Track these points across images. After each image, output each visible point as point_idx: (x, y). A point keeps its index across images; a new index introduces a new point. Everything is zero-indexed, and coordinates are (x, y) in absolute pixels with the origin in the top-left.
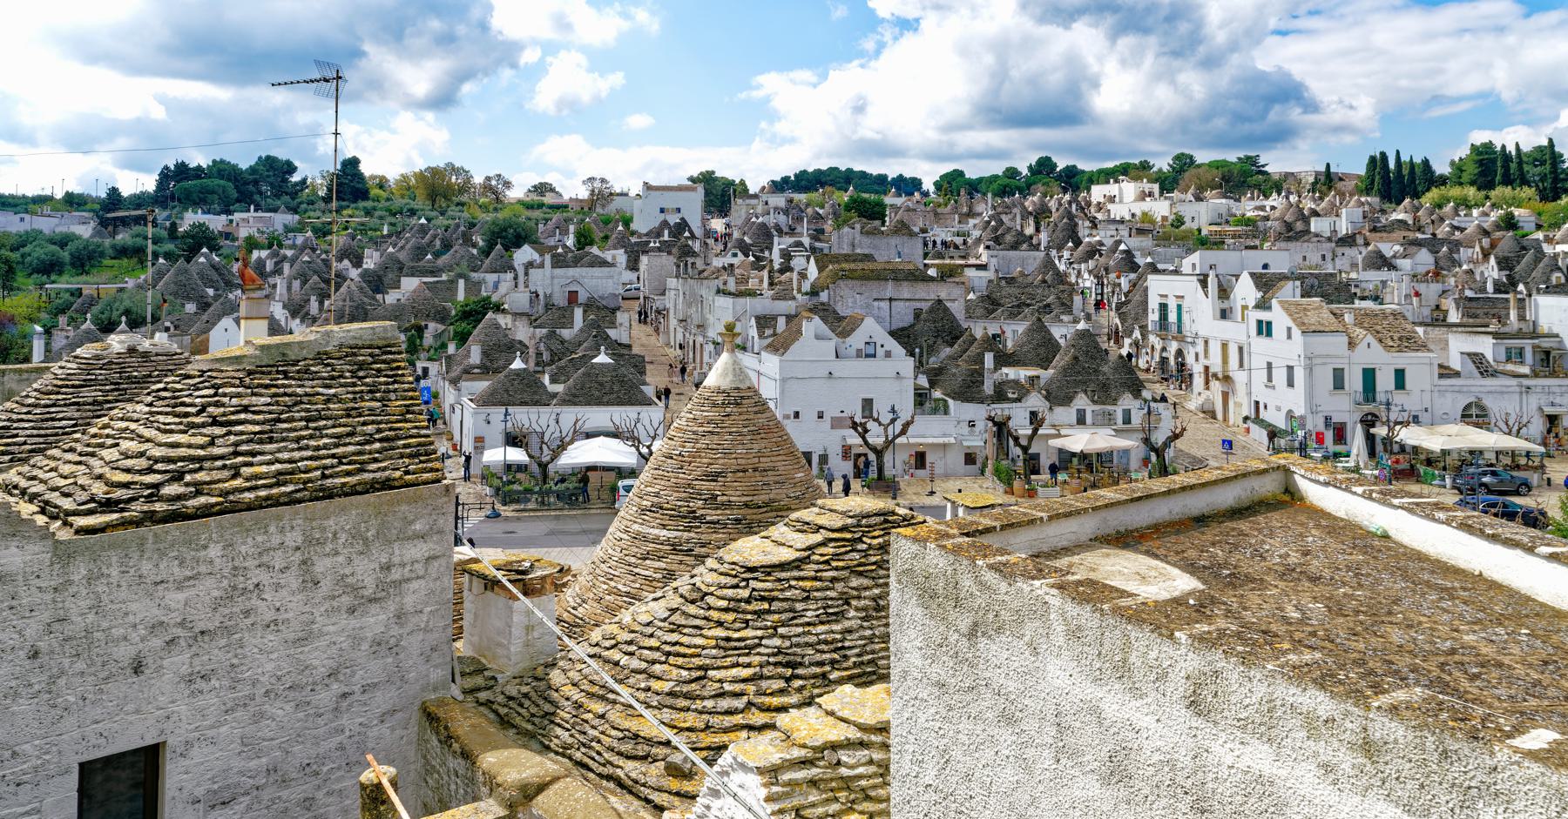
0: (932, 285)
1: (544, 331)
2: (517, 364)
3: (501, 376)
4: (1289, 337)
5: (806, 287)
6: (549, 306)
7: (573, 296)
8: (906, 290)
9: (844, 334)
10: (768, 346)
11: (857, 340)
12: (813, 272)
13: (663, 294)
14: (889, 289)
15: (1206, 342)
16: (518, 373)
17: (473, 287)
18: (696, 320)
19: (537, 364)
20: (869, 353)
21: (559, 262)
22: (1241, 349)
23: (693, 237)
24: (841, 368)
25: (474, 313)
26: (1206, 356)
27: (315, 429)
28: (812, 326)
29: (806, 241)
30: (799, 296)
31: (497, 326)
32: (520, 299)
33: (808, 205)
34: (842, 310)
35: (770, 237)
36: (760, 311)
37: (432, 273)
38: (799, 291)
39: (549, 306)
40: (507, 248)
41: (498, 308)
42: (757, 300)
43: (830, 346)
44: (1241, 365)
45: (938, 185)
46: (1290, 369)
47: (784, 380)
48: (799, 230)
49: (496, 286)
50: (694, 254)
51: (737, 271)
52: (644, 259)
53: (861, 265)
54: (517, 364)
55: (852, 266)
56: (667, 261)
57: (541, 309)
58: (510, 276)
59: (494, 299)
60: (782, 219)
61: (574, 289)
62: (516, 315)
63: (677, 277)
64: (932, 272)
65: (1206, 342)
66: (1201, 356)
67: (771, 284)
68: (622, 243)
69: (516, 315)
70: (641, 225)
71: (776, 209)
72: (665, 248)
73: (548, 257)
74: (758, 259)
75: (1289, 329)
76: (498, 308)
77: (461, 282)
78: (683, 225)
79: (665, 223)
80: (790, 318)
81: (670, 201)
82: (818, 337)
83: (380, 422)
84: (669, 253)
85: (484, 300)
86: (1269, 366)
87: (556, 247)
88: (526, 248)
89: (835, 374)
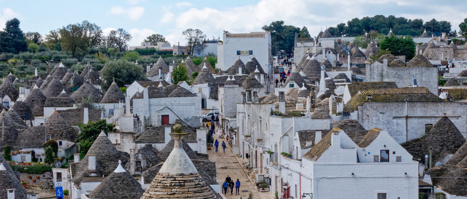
0: (441, 106)
1: (143, 145)
2: (119, 169)
3: (108, 178)
5: (340, 108)
6: (148, 126)
7: (165, 119)
8: (419, 110)
9: (364, 145)
10: (308, 154)
11: (374, 148)
12: (347, 97)
13: (235, 117)
14: (405, 109)
16: (120, 176)
17: (94, 113)
18: (256, 136)
19: (137, 170)
20: (384, 157)
21: (154, 93)
23: (261, 71)
24: (360, 170)
25: (91, 134)
29: (349, 74)
30: (334, 116)
31: (108, 142)
32: (126, 123)
33: (352, 46)
34: (367, 126)
35: (319, 70)
36: (303, 128)
37: (66, 104)
38: (334, 111)
39: (148, 126)
40: (121, 84)
41: (111, 129)
42: (301, 119)
43: (354, 152)
45: (462, 26)
47: (317, 180)
48: (344, 65)
49: (112, 113)
50: (259, 86)
51: (286, 98)
52: (221, 90)
53: (383, 91)
54: (119, 169)
55: (377, 92)
56: (238, 91)
57: (142, 128)
58: (120, 105)
59: (109, 122)
60: (332, 58)
61: (165, 113)
62: (124, 134)
63: (244, 103)
64: (443, 96)
67: (313, 107)
68: (207, 79)
69: (124, 134)
70: (223, 64)
71: (327, 49)
72: (238, 82)
74: (308, 88)
76: (111, 129)
77: (86, 110)
78: (254, 64)
79: (240, 63)
80: (325, 133)
81: (244, 45)
82: (343, 147)
84: (240, 85)
85: (101, 123)
87: (157, 83)
88: (135, 83)
89: (357, 175)
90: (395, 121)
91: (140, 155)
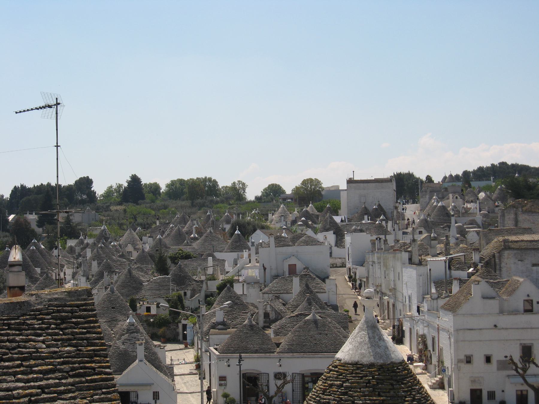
7: (292, 270)
27: (27, 366)
28: (479, 288)
73: (272, 240)
83: (74, 363)
90: (535, 268)
91: (268, 306)
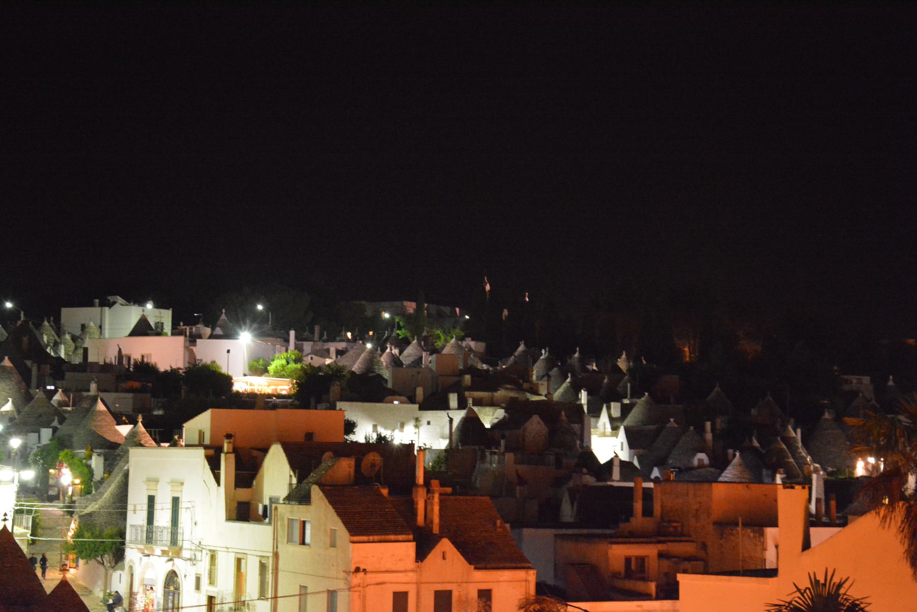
4: (333, 545)
15: (213, 558)
22: (263, 567)
26: (212, 582)
44: (262, 595)
46: (332, 594)
65: (213, 558)
66: (205, 581)
75: (333, 532)
86: (304, 588)
